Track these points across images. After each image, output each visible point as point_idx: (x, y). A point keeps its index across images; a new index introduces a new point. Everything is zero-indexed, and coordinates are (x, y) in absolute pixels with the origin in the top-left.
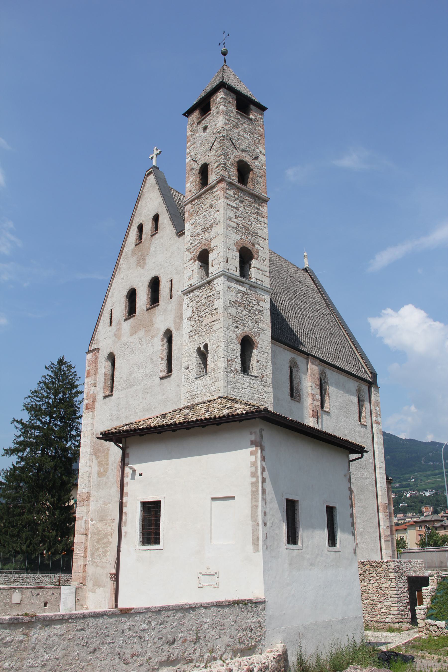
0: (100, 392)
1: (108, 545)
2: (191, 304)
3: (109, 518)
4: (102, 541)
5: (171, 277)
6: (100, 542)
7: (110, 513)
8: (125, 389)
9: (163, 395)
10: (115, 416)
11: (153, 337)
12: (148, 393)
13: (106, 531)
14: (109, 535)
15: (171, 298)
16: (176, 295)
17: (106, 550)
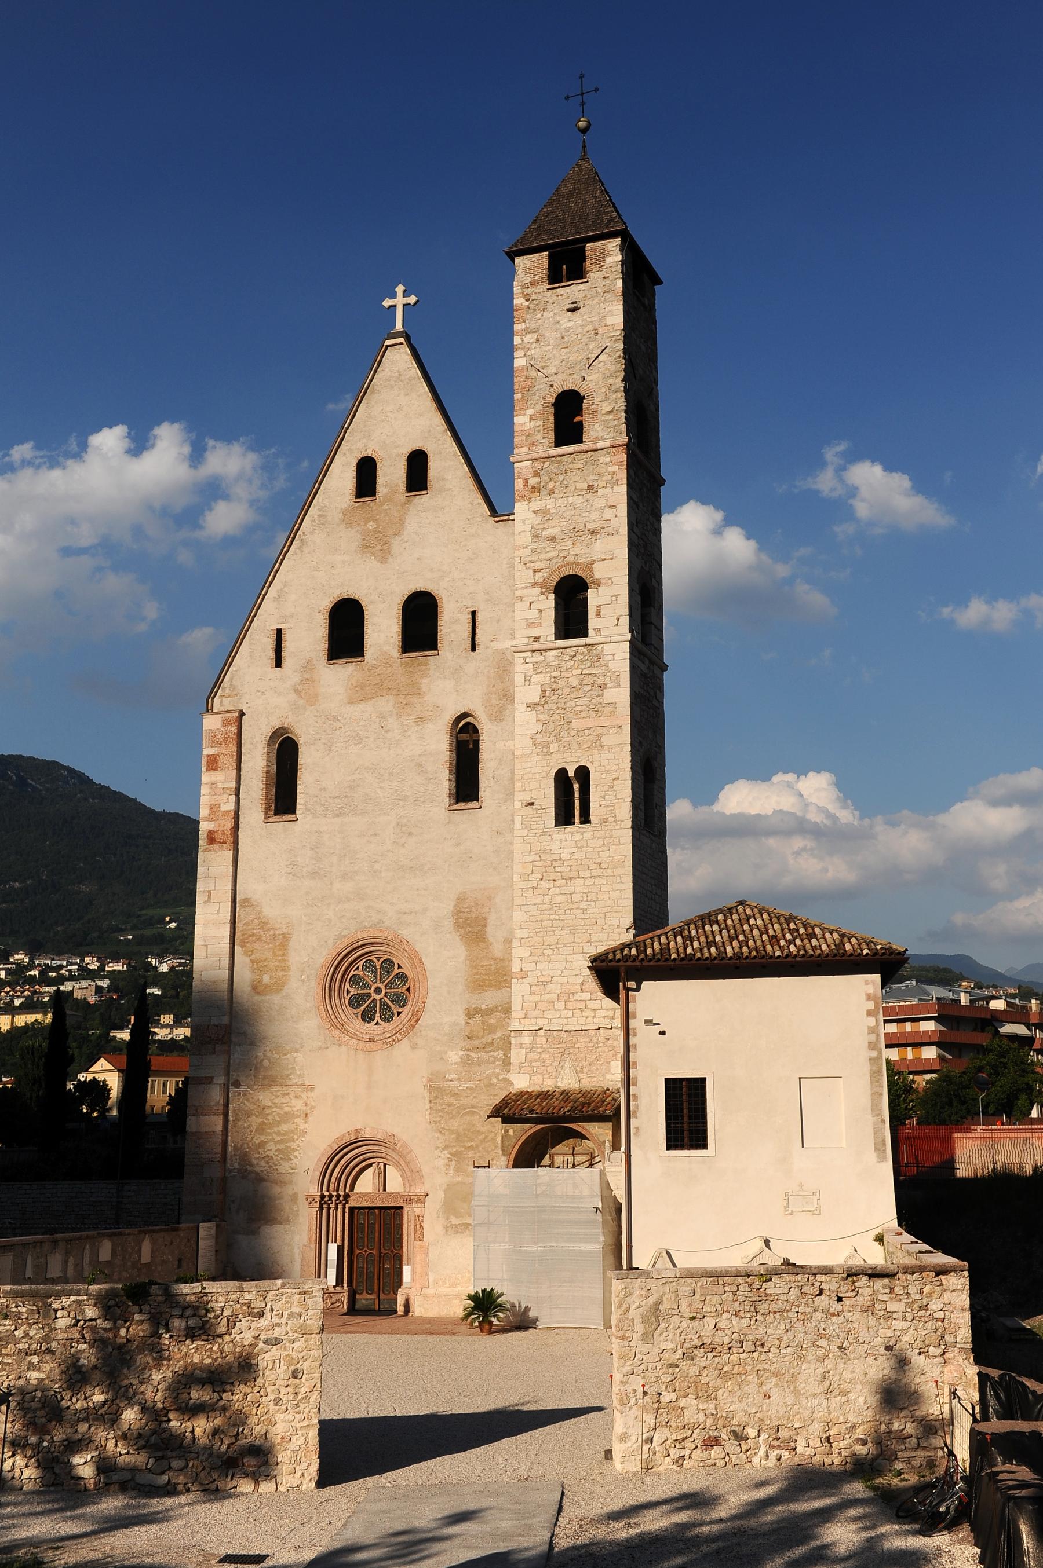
0: (250, 809)
1: (296, 1137)
2: (536, 678)
3: (294, 1081)
4: (276, 1129)
5: (472, 606)
6: (269, 1131)
7: (298, 1072)
8: (337, 816)
9: (458, 845)
10: (305, 870)
11: (420, 720)
12: (410, 834)
13: (287, 1109)
14: (299, 1116)
15: (474, 649)
16: (488, 647)
17: (287, 1147)
